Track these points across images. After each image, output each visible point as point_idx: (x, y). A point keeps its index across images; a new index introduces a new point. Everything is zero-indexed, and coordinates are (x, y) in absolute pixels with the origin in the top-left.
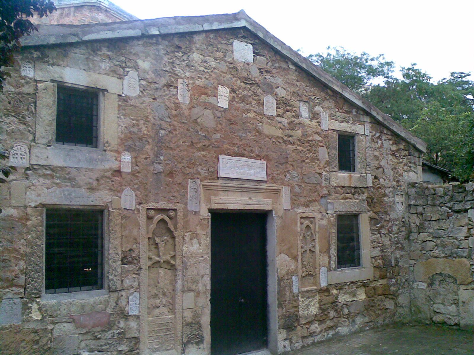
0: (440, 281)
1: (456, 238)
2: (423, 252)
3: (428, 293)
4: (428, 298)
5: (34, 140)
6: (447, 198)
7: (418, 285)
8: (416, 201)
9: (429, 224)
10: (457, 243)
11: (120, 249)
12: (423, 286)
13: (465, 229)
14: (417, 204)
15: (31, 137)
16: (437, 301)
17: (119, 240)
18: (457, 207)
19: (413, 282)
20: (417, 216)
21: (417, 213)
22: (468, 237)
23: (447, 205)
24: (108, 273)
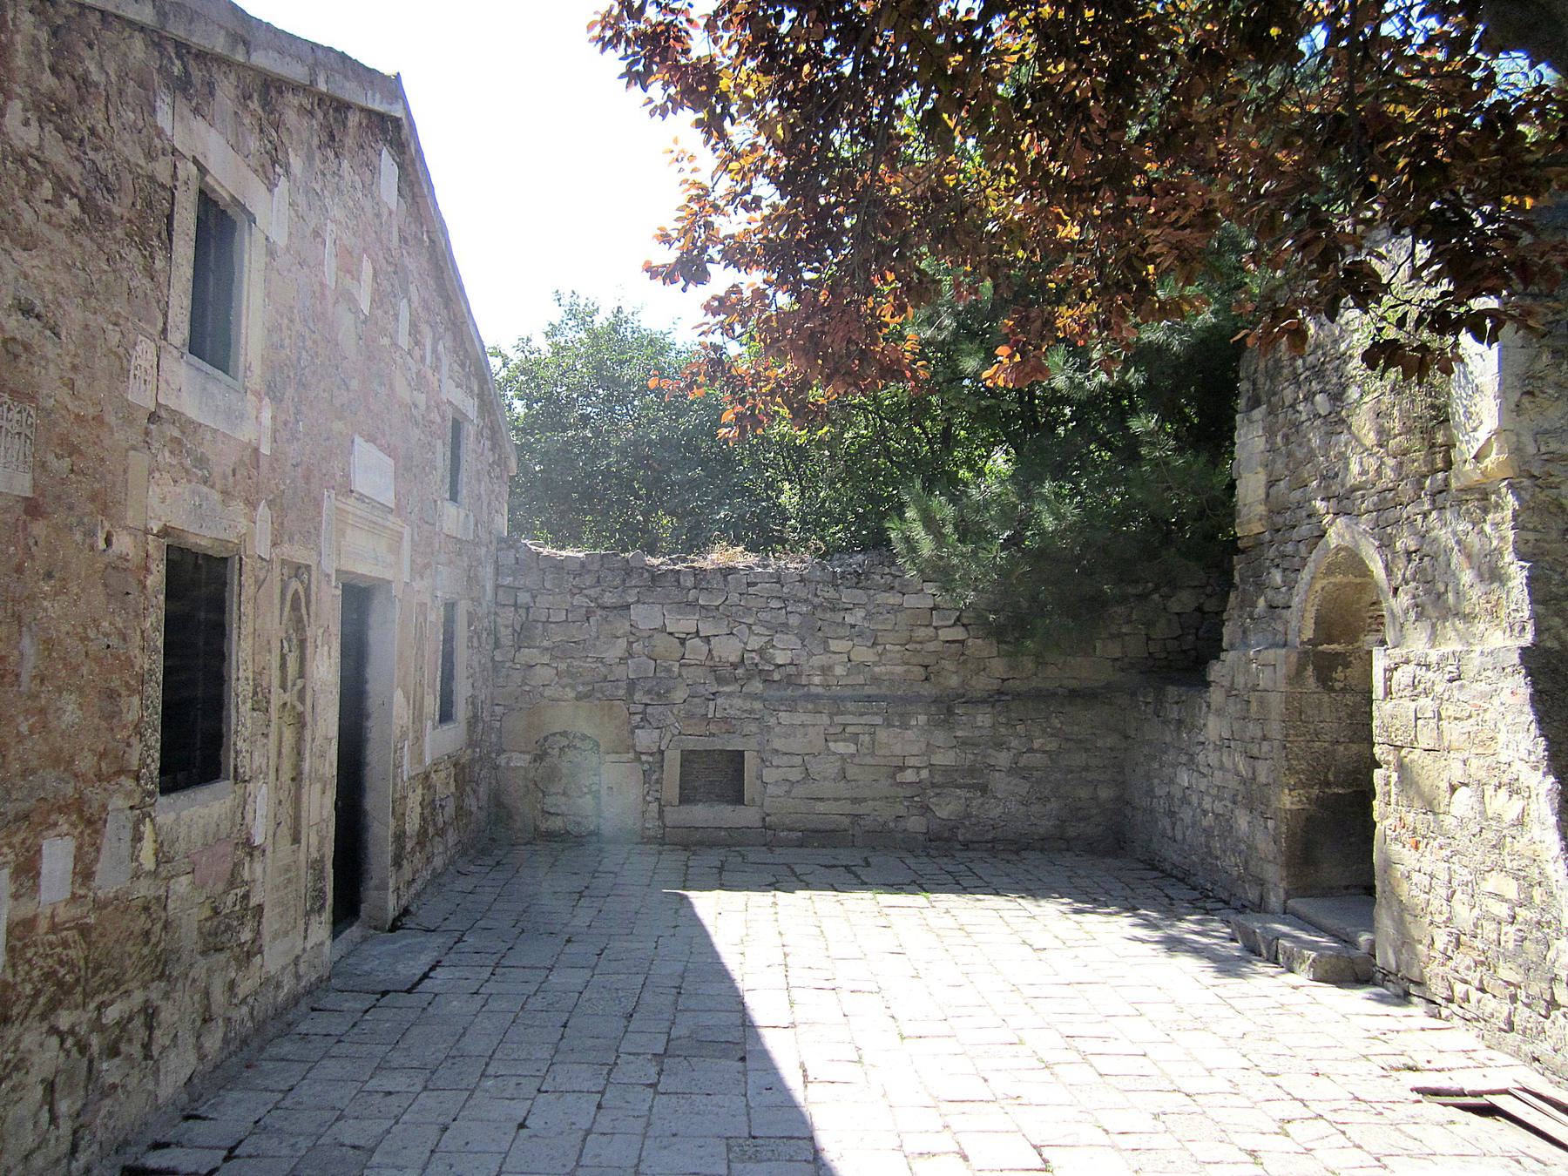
0: (561, 749)
1: (600, 660)
2: (527, 688)
3: (532, 774)
4: (532, 786)
5: (164, 331)
6: (589, 580)
7: (510, 759)
8: (515, 578)
9: (545, 630)
10: (603, 670)
11: (251, 670)
12: (520, 760)
13: (623, 643)
14: (517, 584)
15: (160, 325)
16: (553, 790)
17: (250, 640)
18: (608, 599)
19: (498, 755)
20: (516, 610)
21: (515, 605)
22: (627, 659)
23: (585, 592)
24: (237, 732)
